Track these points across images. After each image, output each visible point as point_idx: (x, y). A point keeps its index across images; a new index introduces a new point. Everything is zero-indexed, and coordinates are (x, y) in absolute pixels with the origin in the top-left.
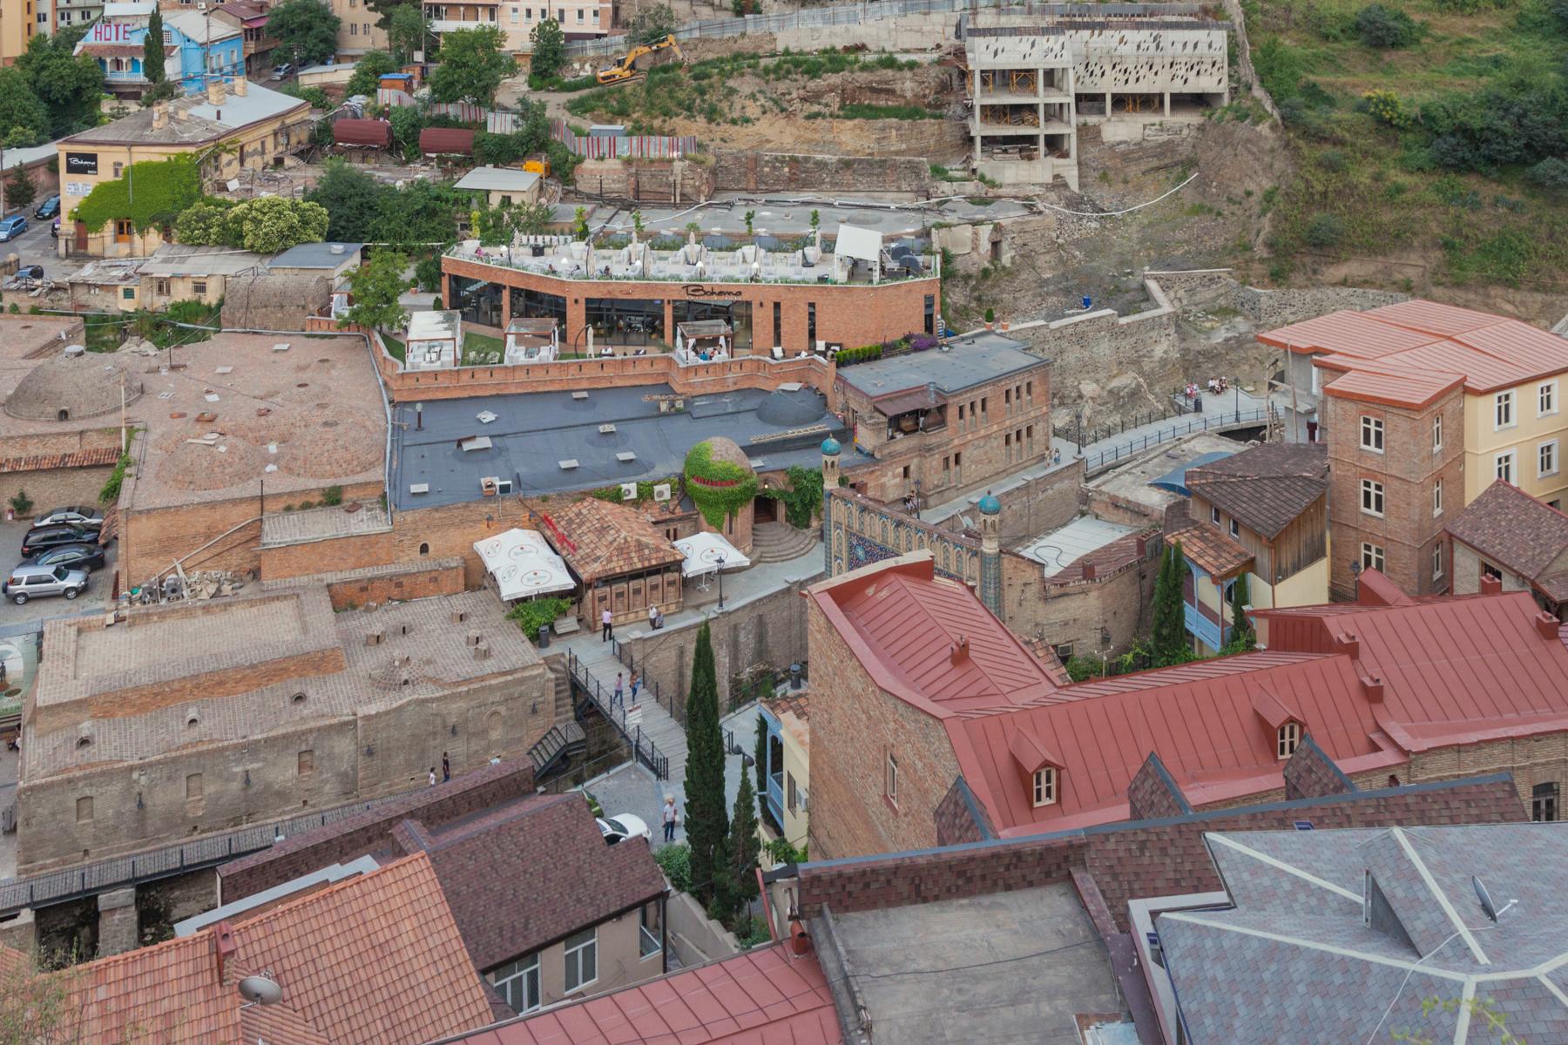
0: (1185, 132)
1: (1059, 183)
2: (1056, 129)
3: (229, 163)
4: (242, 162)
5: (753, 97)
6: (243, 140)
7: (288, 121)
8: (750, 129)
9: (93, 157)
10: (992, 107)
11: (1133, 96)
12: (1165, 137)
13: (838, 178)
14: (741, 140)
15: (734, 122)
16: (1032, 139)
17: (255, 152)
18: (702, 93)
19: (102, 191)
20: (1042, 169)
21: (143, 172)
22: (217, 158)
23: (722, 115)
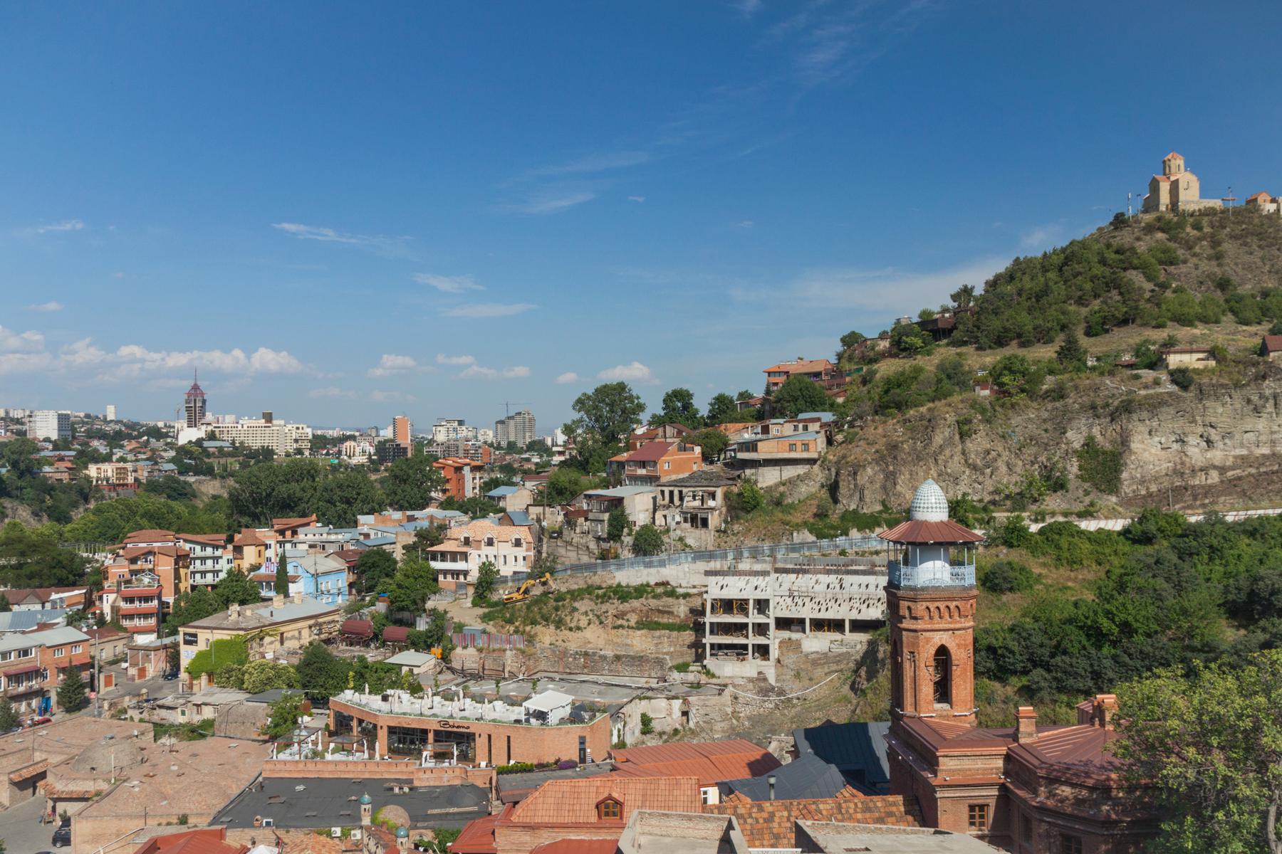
0: (859, 647)
1: (761, 677)
2: (761, 640)
3: (272, 643)
4: (282, 643)
5: (586, 613)
6: (283, 629)
7: (320, 620)
8: (579, 634)
9: (195, 635)
10: (719, 624)
11: (829, 620)
12: (844, 650)
13: (613, 666)
14: (573, 642)
15: (571, 629)
16: (745, 647)
17: (293, 637)
18: (557, 609)
19: (200, 655)
20: (751, 667)
21: (220, 644)
22: (262, 639)
23: (565, 624)
